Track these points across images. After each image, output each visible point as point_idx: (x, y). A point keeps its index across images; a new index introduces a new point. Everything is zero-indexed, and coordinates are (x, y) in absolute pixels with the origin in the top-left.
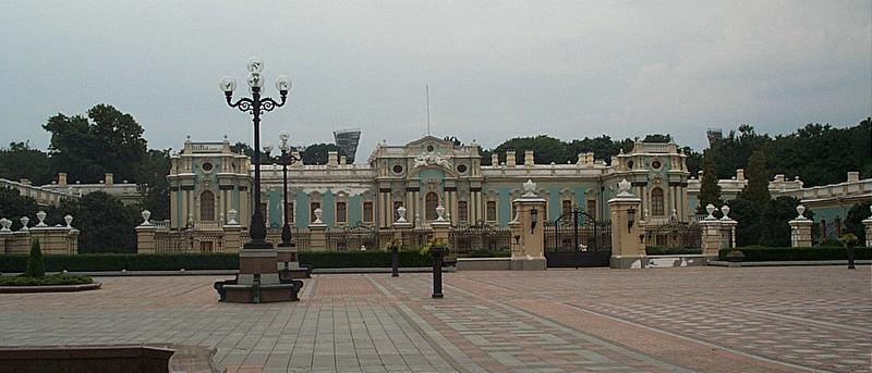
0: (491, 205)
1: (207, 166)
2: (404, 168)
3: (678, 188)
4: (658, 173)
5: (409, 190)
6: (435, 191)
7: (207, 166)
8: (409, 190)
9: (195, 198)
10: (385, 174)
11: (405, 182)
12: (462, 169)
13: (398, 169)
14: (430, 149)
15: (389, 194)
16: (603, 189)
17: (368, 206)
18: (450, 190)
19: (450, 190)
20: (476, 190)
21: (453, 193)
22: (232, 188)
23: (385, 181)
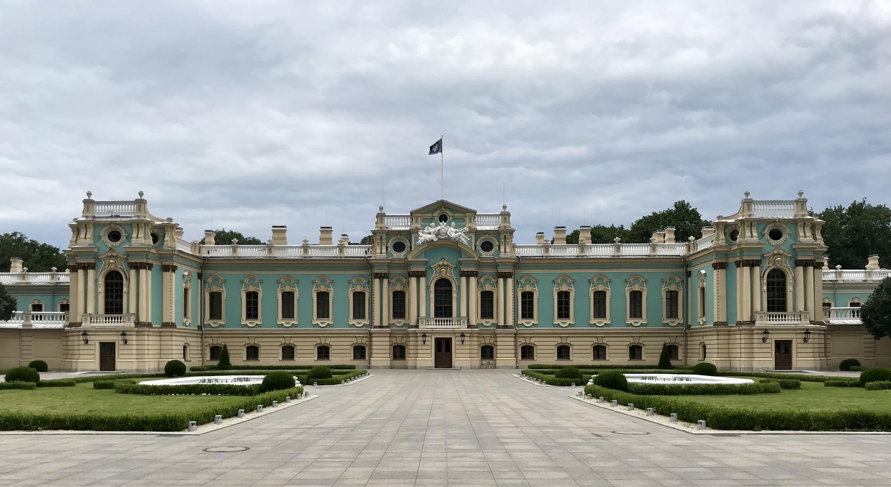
0: (528, 298)
1: (115, 236)
2: (407, 244)
3: (811, 269)
4: (777, 247)
5: (411, 274)
7: (115, 236)
9: (96, 281)
10: (380, 253)
11: (406, 264)
12: (487, 246)
13: (399, 247)
14: (443, 218)
16: (689, 274)
17: (359, 298)
18: (468, 275)
20: (505, 276)
21: (473, 280)
22: (149, 267)
23: (380, 263)
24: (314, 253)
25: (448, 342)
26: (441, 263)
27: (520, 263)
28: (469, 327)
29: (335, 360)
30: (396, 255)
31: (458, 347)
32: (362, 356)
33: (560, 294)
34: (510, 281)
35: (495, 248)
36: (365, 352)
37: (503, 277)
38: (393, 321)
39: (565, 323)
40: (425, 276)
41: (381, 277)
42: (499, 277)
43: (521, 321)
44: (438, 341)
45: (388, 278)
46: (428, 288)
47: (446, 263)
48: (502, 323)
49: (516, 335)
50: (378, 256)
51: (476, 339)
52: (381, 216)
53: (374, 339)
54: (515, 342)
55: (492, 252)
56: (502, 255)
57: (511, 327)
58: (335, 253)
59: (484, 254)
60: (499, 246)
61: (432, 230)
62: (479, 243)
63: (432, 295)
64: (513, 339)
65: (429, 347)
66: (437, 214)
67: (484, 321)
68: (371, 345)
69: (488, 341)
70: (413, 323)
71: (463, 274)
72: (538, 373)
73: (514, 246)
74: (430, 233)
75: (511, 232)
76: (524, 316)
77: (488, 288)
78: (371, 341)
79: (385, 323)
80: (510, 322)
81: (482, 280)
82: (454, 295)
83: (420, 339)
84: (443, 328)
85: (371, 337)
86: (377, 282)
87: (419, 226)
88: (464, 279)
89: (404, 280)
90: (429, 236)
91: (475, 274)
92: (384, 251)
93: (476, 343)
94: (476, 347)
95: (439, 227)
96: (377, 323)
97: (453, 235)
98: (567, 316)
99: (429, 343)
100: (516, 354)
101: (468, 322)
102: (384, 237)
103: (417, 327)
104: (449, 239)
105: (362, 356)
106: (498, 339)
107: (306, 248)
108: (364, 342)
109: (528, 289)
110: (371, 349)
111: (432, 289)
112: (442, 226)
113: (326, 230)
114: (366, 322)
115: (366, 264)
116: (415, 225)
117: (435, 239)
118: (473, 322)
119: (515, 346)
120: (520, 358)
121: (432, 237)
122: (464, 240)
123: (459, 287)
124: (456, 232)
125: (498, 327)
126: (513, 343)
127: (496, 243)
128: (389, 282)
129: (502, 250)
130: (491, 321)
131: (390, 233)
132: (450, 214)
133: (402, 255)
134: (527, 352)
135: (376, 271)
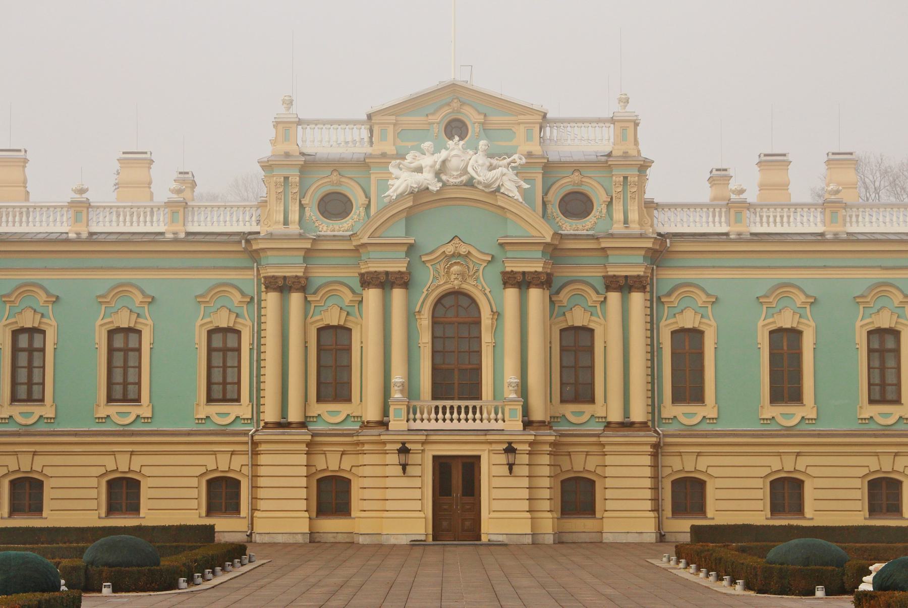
2: (358, 198)
5: (368, 280)
6: (468, 287)
8: (368, 280)
13: (335, 205)
14: (456, 128)
15: (296, 299)
17: (223, 345)
18: (521, 282)
19: (521, 282)
24: (103, 224)
25: (471, 465)
26: (450, 249)
27: (661, 251)
28: (528, 424)
29: (155, 512)
30: (326, 227)
31: (497, 482)
32: (233, 508)
33: (777, 334)
34: (637, 299)
35: (599, 208)
36: (237, 495)
37: (619, 289)
38: (316, 409)
39: (789, 415)
40: (406, 285)
41: (283, 286)
42: (608, 288)
43: (669, 410)
44: (442, 465)
45: (303, 289)
46: (411, 316)
47: (463, 250)
48: (615, 416)
49: (657, 450)
50: (279, 229)
51: (546, 459)
52: (286, 127)
53: (263, 459)
54: (655, 466)
55: (590, 220)
56: (618, 228)
57: (644, 425)
58: (159, 225)
59: (569, 226)
60: (610, 204)
61: (427, 161)
62: (555, 197)
63: (425, 338)
64: (647, 460)
65: (417, 482)
66: (441, 117)
67: (569, 410)
68: (255, 476)
69: (581, 463)
70: (372, 414)
71: (511, 280)
72: (716, 549)
73: (650, 206)
74: (419, 170)
75: (644, 166)
76: (678, 398)
77: (578, 318)
78: (255, 465)
79: (294, 416)
80: (638, 414)
81: (564, 296)
82: (486, 337)
83: (393, 458)
84: (451, 431)
85: (255, 453)
86: (271, 299)
87: (390, 149)
88: (511, 294)
89: (348, 296)
90: (419, 177)
91: (545, 281)
92: (294, 216)
93: (546, 471)
94: (546, 482)
95: (444, 154)
96: (270, 414)
97: (483, 176)
98: (796, 397)
99: (416, 471)
100: (656, 501)
101: (526, 411)
102: (295, 179)
103: (383, 424)
104: (470, 184)
105: (233, 508)
106: (609, 460)
107: (81, 207)
108: (235, 465)
109: (688, 321)
110: (254, 487)
111: (425, 321)
112: (455, 147)
113: (137, 160)
114: (243, 409)
115: (247, 247)
116: (377, 149)
117: (435, 186)
118: (538, 414)
119: (655, 478)
120: (668, 511)
121: (427, 178)
122: (511, 186)
123: (497, 315)
124: (491, 168)
125: (609, 425)
126: (648, 472)
127: (599, 198)
128: (307, 302)
129: (618, 215)
130: (587, 408)
131: (309, 165)
132: (471, 117)
133: (342, 227)
134: (689, 494)
135: (271, 272)
